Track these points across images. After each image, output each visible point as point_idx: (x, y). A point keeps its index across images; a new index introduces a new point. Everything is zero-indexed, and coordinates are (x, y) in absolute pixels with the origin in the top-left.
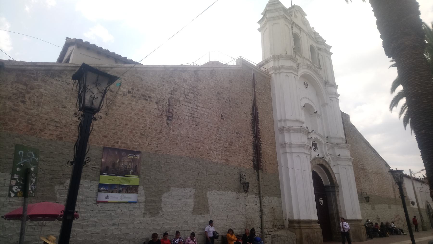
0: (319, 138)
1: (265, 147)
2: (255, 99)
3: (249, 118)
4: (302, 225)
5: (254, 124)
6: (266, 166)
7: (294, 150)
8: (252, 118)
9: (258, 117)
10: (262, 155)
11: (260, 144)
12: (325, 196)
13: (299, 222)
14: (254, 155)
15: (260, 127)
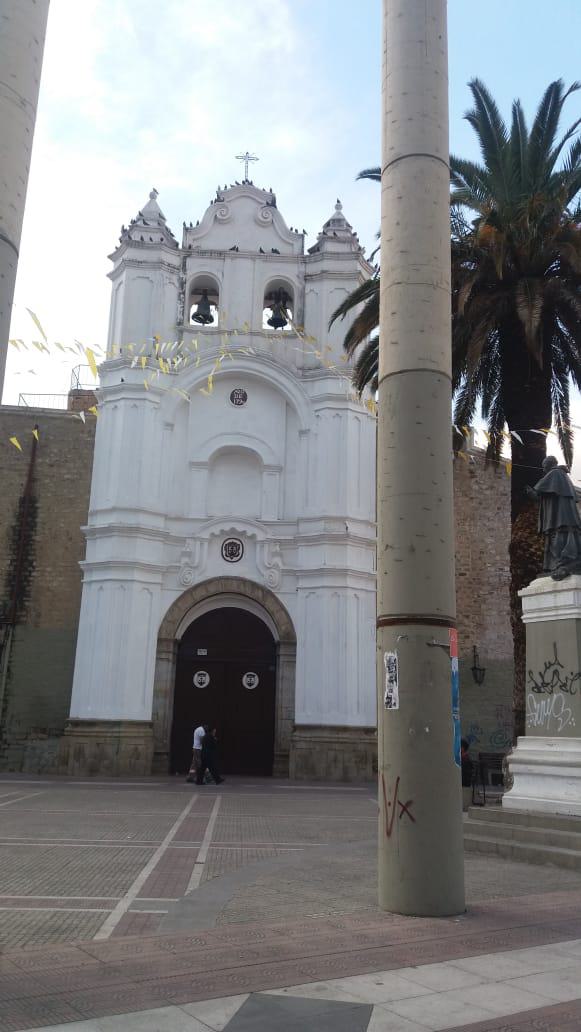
0: (240, 528)
1: (46, 577)
2: (31, 479)
3: (6, 523)
4: (79, 729)
5: (19, 535)
6: (39, 615)
7: (95, 576)
8: (14, 524)
9: (35, 517)
10: (32, 594)
11: (30, 572)
12: (272, 668)
13: (78, 723)
14: (6, 598)
15: (37, 538)
